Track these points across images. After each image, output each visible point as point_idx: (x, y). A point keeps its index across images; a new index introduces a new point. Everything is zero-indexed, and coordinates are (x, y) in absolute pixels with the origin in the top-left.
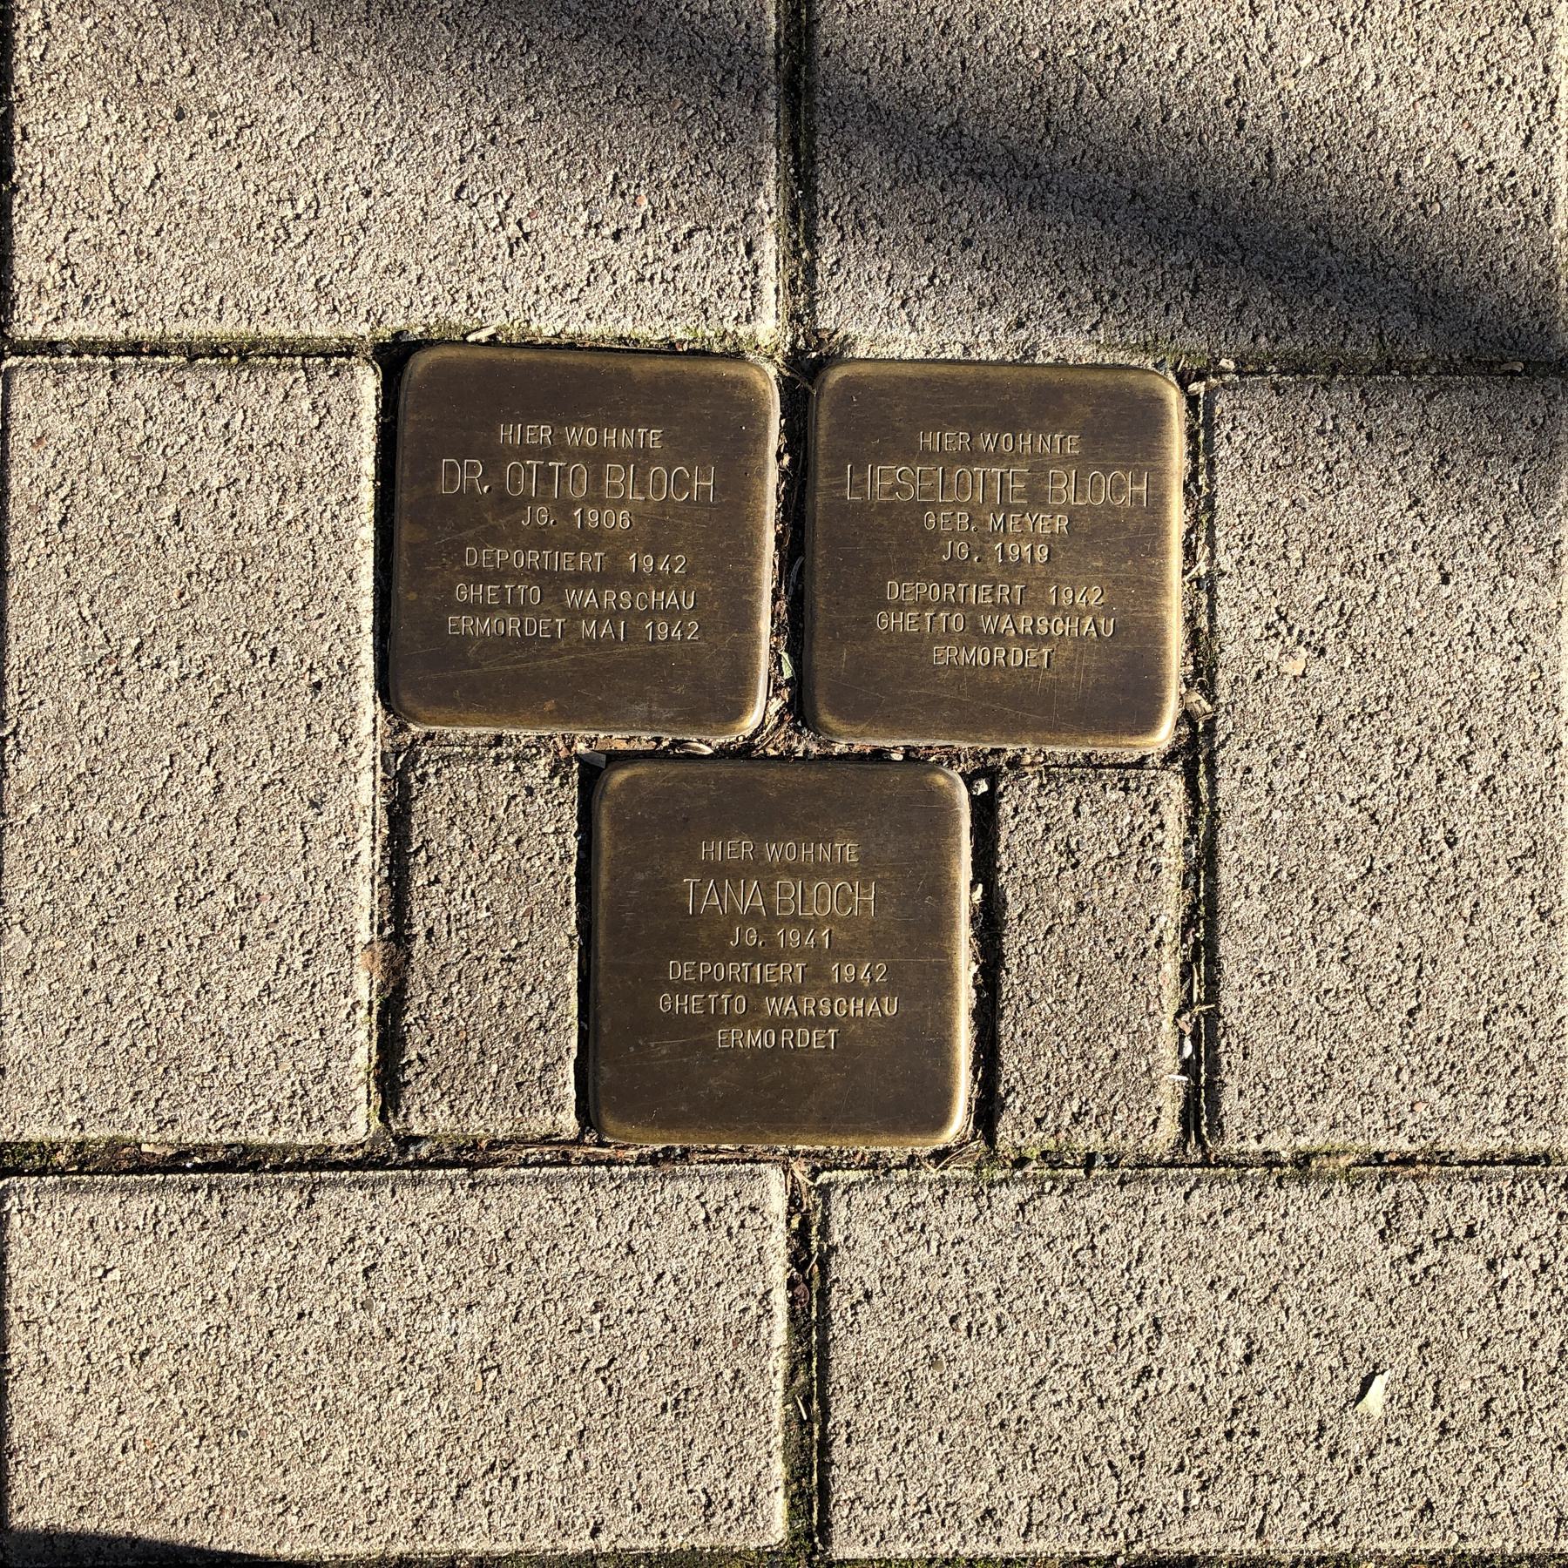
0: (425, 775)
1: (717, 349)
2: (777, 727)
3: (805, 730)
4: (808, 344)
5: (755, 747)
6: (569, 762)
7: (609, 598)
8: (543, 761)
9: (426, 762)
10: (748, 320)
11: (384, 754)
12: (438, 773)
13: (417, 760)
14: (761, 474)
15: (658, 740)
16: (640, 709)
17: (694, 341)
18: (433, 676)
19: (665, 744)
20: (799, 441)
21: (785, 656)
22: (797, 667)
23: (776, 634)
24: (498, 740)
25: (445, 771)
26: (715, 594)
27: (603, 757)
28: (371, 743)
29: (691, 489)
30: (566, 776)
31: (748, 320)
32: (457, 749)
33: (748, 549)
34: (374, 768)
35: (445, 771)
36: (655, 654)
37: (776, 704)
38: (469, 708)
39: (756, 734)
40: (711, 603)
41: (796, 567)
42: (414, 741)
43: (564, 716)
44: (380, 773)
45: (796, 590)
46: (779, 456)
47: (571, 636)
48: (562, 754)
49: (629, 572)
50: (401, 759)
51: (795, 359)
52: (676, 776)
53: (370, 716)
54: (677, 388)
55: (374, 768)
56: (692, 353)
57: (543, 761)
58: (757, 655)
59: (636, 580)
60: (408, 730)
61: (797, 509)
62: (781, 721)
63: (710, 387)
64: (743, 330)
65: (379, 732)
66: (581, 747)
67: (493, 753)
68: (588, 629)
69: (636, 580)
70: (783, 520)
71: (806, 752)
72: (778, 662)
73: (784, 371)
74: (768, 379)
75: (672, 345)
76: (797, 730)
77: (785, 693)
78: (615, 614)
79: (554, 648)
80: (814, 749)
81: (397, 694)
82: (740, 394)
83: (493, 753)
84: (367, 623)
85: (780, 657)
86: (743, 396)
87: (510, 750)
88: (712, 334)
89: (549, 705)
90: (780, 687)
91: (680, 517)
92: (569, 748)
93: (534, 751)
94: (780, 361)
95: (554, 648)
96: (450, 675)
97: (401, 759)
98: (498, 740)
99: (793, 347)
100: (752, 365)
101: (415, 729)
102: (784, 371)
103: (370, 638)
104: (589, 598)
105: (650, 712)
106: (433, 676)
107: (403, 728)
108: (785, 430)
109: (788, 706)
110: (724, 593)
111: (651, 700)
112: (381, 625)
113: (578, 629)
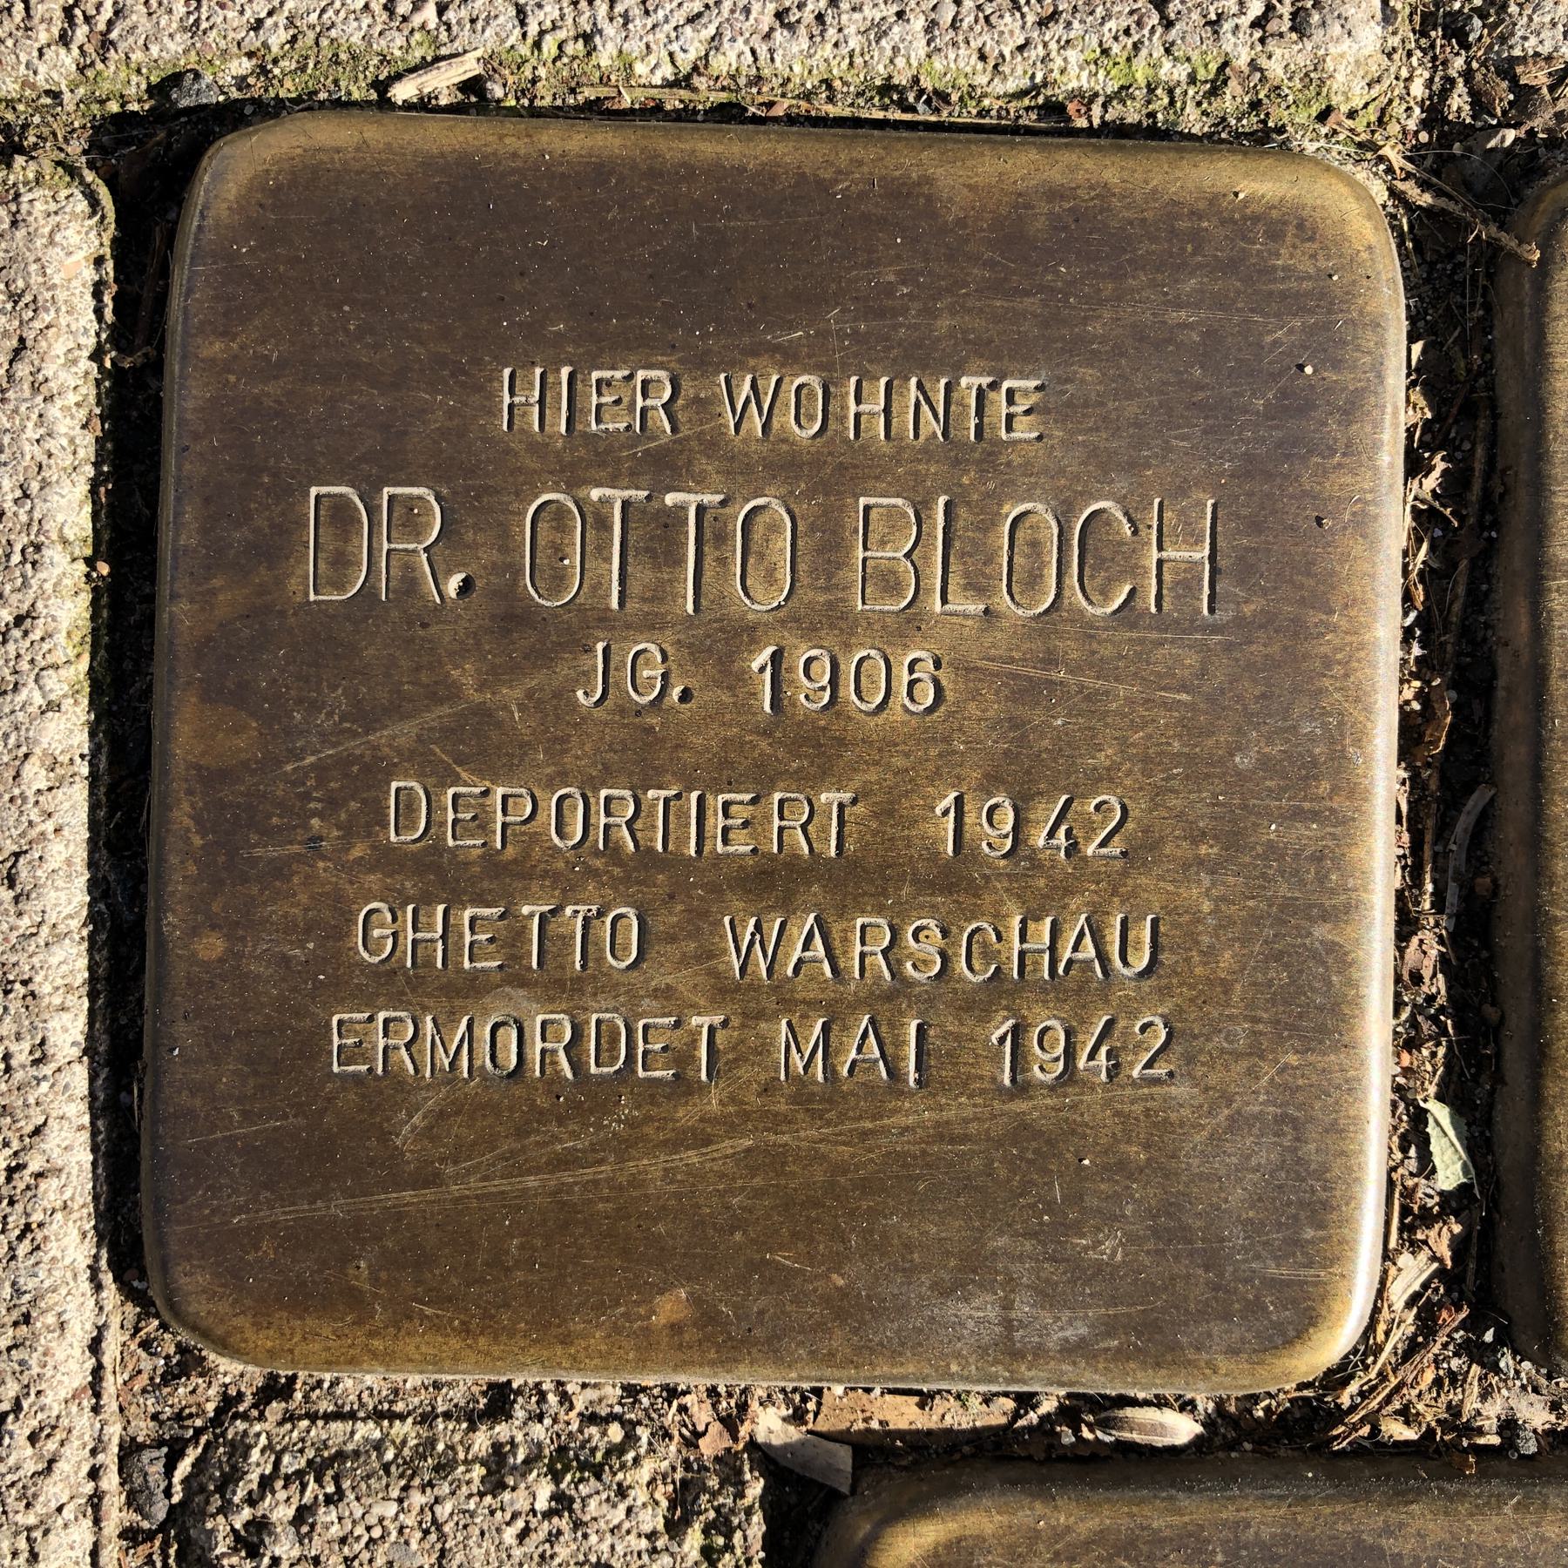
0: (260, 1526)
1: (1193, 121)
2: (1412, 1349)
3: (1506, 1361)
4: (1479, 102)
5: (1339, 1415)
6: (728, 1466)
7: (866, 940)
8: (645, 1473)
9: (266, 1483)
10: (1299, 24)
11: (130, 1450)
12: (303, 1515)
13: (234, 1476)
14: (1363, 523)
15: (1026, 1401)
16: (978, 1312)
17: (1123, 94)
18: (283, 1215)
19: (1048, 1406)
20: (1469, 411)
21: (1440, 1113)
22: (1477, 1146)
23: (1408, 1042)
24: (499, 1402)
25: (327, 1515)
26: (1225, 923)
27: (844, 1456)
28: (84, 1424)
29: (1134, 571)
30: (722, 1525)
31: (1299, 24)
32: (367, 1430)
33: (1313, 778)
34: (96, 1501)
35: (327, 1515)
36: (1023, 1130)
37: (1412, 1272)
38: (402, 1317)
39: (1337, 1377)
40: (1210, 954)
41: (1464, 823)
42: (228, 1402)
43: (713, 1336)
44: (116, 1515)
45: (1468, 895)
46: (1415, 466)
47: (744, 1072)
48: (710, 1447)
49: (935, 856)
50: (184, 1467)
51: (1443, 149)
52: (1100, 1537)
53: (80, 1331)
54: (1092, 240)
55: (96, 1501)
56: (1117, 132)
57: (645, 1473)
58: (1358, 1121)
59: (955, 881)
60: (207, 1373)
61: (1466, 631)
62: (1427, 1323)
63: (1197, 237)
64: (1282, 60)
65: (110, 1385)
66: (770, 1425)
67: (481, 1442)
68: (792, 1048)
69: (955, 881)
70: (1423, 668)
71: (1509, 1426)
72: (1414, 1135)
73: (1411, 190)
74: (1357, 213)
75: (1054, 109)
76: (1483, 1356)
77: (1440, 1239)
78: (890, 996)
79: (685, 1115)
80: (1536, 1415)
81: (164, 1267)
82: (1291, 257)
83: (481, 1442)
84: (69, 1029)
85: (1419, 1117)
86: (1307, 266)
87: (539, 1431)
88: (1181, 73)
89: (671, 1306)
90: (1427, 1218)
91: (1101, 668)
92: (730, 1424)
93: (616, 1433)
94: (1397, 161)
95: (685, 1115)
96: (337, 1208)
97: (184, 1467)
98: (499, 1402)
99: (1434, 114)
100: (1318, 163)
101: (228, 1368)
102: (1411, 190)
103: (79, 1078)
104: (801, 941)
105: (1008, 1324)
106: (283, 1215)
107: (187, 1364)
108: (1424, 377)
109: (1451, 1280)
110: (1255, 919)
111: (1011, 1283)
112: (115, 1033)
113: (764, 1048)
